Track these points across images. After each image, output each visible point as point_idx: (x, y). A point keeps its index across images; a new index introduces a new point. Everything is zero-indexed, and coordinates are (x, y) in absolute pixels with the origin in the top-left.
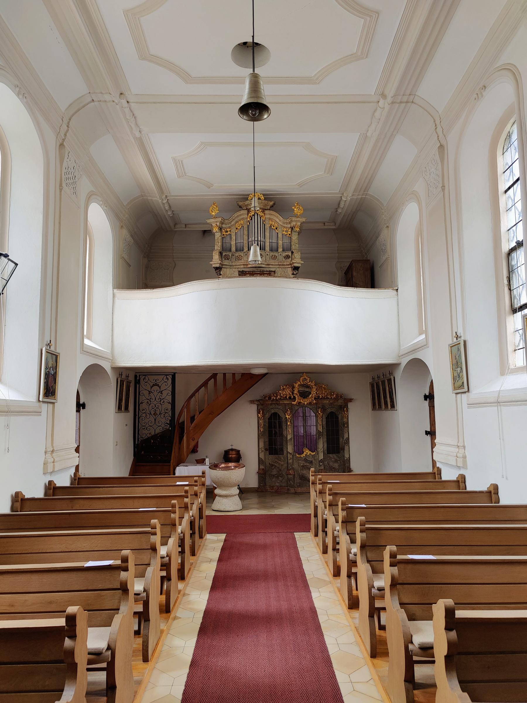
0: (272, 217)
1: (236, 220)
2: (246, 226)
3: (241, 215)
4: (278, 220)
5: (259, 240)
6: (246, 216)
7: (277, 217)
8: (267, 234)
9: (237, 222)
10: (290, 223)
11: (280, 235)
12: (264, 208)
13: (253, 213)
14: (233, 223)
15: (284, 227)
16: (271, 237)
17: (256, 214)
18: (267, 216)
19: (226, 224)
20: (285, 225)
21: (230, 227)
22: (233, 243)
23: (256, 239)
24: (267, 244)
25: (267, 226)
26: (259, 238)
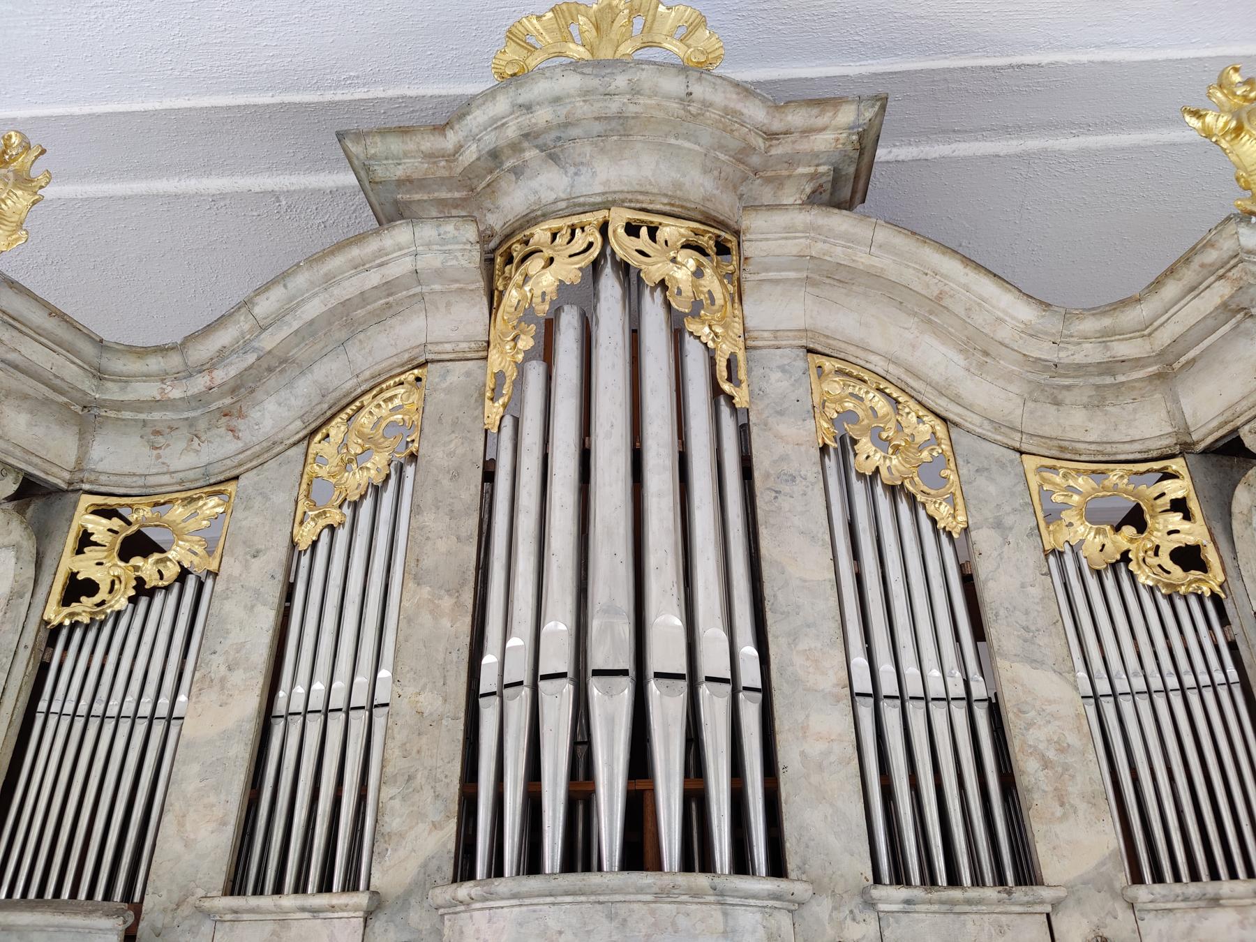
0: (845, 320)
1: (335, 372)
2: (451, 454)
3: (390, 301)
4: (937, 359)
5: (666, 652)
6: (462, 319)
7: (931, 310)
8: (801, 559)
9: (347, 405)
10: (1168, 370)
11: (1010, 580)
12: (725, 205)
13: (569, 270)
14: (274, 414)
15: (1064, 453)
16: (864, 608)
17: (610, 286)
18: (775, 311)
19: (155, 435)
20: (1079, 424)
21: (217, 484)
22: (216, 721)
23: (612, 646)
24: (819, 742)
25: (786, 445)
26: (665, 621)
